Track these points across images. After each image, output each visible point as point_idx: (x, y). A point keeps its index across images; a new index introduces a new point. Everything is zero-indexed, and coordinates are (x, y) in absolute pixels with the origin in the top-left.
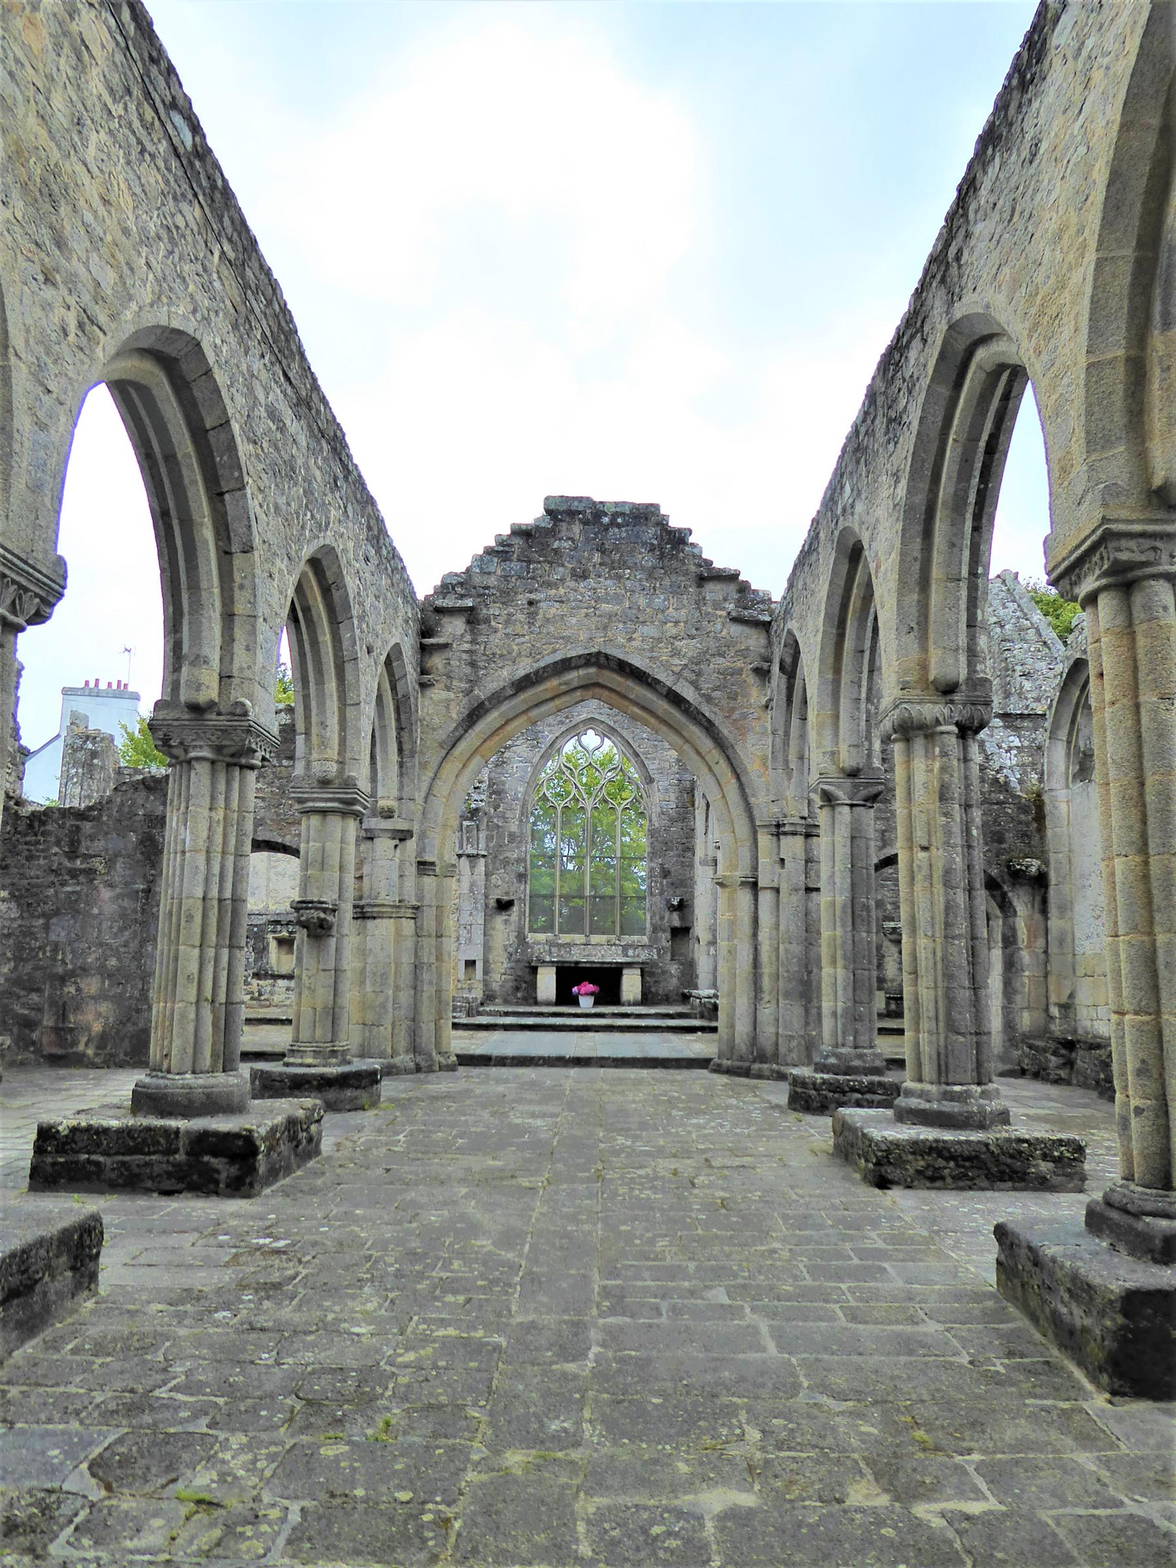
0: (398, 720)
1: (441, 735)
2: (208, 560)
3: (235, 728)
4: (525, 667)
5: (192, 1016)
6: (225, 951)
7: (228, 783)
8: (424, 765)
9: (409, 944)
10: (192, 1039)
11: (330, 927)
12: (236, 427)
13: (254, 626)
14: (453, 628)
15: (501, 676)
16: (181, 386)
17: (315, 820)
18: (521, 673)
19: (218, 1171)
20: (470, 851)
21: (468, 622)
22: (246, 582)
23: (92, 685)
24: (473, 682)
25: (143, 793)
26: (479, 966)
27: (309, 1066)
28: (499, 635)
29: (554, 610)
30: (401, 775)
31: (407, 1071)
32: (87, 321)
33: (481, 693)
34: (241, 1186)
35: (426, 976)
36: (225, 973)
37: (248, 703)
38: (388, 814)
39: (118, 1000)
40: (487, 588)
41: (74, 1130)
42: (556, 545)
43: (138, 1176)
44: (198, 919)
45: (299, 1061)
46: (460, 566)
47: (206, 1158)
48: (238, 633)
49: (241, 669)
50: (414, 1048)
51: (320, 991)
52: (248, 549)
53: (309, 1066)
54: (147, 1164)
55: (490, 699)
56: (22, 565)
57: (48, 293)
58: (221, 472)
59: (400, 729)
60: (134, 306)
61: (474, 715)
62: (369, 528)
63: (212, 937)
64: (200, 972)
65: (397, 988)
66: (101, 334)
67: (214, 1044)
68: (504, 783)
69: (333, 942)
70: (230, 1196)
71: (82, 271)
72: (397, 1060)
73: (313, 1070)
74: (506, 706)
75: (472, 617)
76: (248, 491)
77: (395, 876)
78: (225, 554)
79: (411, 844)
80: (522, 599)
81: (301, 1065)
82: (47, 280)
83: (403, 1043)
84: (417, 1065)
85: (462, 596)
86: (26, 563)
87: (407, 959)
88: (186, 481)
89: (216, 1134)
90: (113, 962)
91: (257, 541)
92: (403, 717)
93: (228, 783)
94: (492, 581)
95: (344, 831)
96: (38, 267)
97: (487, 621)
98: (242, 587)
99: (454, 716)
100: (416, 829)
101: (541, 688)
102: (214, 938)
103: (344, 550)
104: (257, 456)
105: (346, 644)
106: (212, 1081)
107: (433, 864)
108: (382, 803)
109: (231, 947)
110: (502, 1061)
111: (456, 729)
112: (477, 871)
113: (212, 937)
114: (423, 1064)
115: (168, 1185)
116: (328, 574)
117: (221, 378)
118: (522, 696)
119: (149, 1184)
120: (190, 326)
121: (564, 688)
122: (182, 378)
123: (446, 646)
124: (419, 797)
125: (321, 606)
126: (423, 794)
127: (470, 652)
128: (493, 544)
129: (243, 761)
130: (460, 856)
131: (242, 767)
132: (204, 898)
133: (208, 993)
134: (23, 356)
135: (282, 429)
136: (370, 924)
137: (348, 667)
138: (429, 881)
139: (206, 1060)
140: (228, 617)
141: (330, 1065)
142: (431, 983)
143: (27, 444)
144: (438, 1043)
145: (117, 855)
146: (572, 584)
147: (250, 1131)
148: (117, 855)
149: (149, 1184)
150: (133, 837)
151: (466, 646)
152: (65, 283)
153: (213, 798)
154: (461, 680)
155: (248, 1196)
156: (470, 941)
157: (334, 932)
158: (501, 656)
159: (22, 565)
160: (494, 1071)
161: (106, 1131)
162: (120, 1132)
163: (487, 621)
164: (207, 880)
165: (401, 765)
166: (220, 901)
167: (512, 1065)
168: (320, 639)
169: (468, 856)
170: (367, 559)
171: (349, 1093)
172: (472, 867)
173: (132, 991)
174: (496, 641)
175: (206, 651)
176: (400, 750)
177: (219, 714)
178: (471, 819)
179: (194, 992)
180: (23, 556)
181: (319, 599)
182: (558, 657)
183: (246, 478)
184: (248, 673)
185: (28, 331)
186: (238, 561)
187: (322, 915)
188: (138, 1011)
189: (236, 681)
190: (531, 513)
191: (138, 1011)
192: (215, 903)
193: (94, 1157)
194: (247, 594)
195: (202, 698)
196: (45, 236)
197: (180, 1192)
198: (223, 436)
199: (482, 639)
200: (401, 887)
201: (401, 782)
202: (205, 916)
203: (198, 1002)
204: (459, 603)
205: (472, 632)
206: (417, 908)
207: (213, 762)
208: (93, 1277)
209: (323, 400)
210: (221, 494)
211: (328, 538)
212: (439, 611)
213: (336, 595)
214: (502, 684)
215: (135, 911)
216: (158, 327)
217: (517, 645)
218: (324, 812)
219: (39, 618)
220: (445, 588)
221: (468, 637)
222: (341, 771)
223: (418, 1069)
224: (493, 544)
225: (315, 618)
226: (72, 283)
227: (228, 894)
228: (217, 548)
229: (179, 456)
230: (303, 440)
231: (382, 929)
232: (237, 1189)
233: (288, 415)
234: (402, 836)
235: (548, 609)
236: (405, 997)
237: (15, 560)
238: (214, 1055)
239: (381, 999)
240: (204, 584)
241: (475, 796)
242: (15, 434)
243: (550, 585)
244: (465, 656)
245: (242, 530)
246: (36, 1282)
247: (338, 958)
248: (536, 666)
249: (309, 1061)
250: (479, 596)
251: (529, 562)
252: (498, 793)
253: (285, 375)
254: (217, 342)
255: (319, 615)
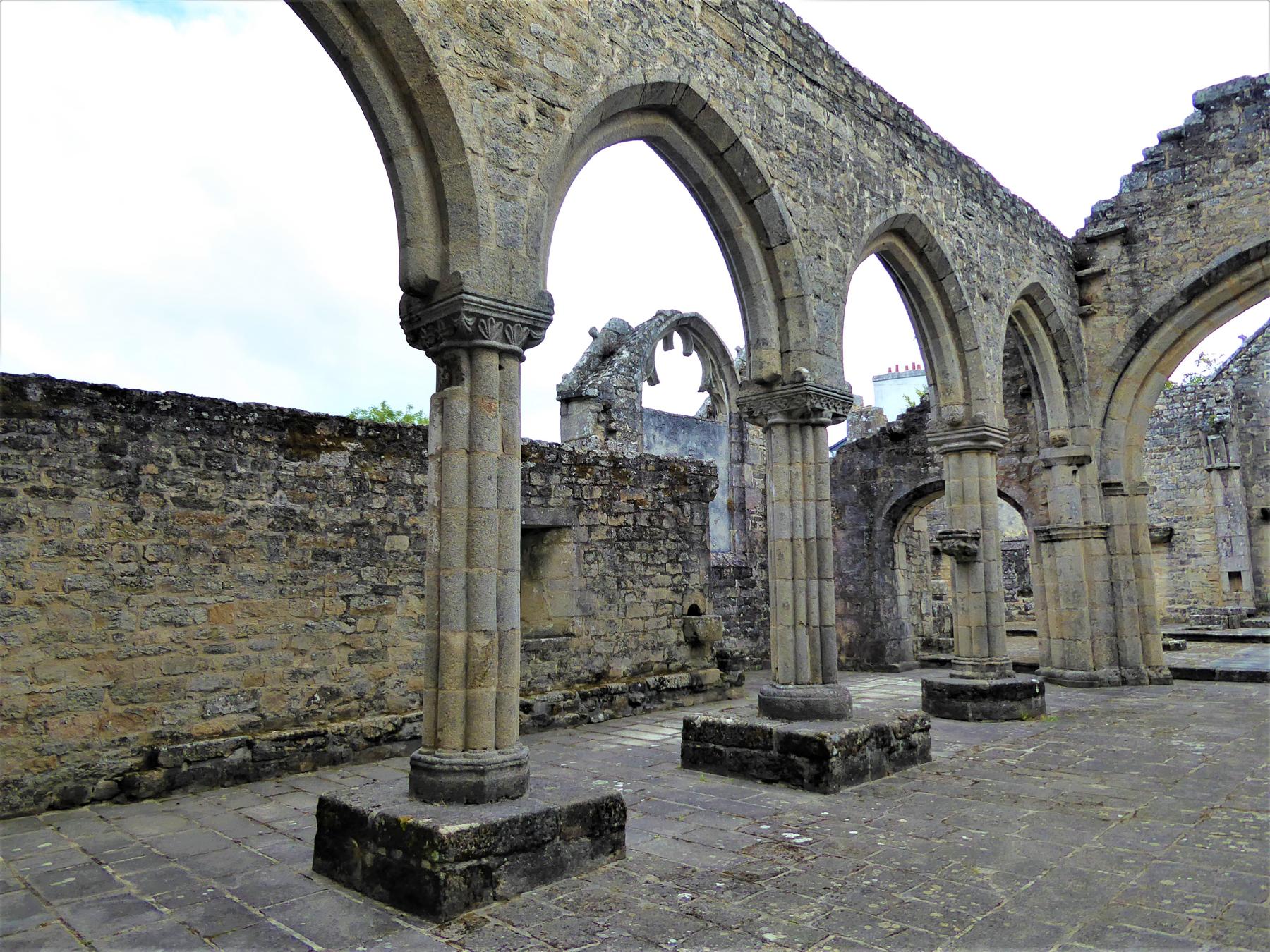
0: (1057, 354)
1: (1110, 359)
2: (753, 259)
3: (796, 394)
4: (1193, 273)
5: (791, 636)
6: (814, 585)
7: (803, 442)
8: (1095, 392)
9: (1102, 563)
10: (792, 656)
11: (975, 554)
12: (748, 143)
13: (803, 304)
14: (1109, 253)
15: (1167, 289)
16: (688, 126)
17: (953, 459)
18: (1190, 280)
19: (801, 768)
20: (1219, 464)
21: (1124, 244)
22: (790, 269)
23: (894, 370)
24: (1137, 302)
25: (858, 453)
26: (1247, 579)
27: (968, 678)
28: (1159, 248)
29: (1221, 205)
30: (1070, 404)
31: (1111, 683)
32: (546, 108)
33: (1147, 310)
34: (819, 782)
35: (1124, 593)
36: (816, 601)
37: (805, 370)
38: (1062, 443)
39: (858, 618)
40: (1141, 204)
41: (705, 724)
42: (1212, 138)
43: (746, 765)
44: (788, 556)
45: (960, 673)
46: (1110, 190)
47: (792, 757)
48: (791, 314)
49: (797, 343)
50: (1119, 661)
51: (973, 611)
52: (785, 241)
53: (968, 678)
54: (752, 756)
55: (1158, 314)
56: (502, 305)
57: (501, 98)
58: (745, 184)
59: (1061, 362)
60: (601, 79)
61: (1144, 334)
62: (967, 185)
63: (802, 571)
64: (795, 601)
65: (1093, 605)
66: (565, 113)
67: (812, 661)
68: (1254, 392)
69: (980, 567)
70: (812, 790)
71: (537, 70)
72: (1101, 673)
73: (967, 682)
74: (1179, 318)
75: (1127, 238)
76: (775, 192)
77: (1077, 500)
78: (768, 250)
79: (1092, 470)
80: (1180, 205)
81: (962, 677)
82: (498, 88)
83: (1105, 656)
84: (1123, 677)
85: (1114, 220)
86: (505, 303)
87: (1100, 579)
88: (718, 200)
89: (797, 737)
90: (851, 588)
91: (794, 230)
92: (1061, 349)
93: (803, 442)
94: (1145, 196)
95: (981, 466)
96: (487, 82)
97: (1144, 237)
98: (786, 274)
99: (1121, 338)
100: (1094, 453)
101: (1219, 289)
102: (803, 572)
103: (933, 214)
104: (782, 159)
105: (952, 297)
106: (811, 691)
107: (1119, 484)
108: (1053, 434)
109: (820, 578)
110: (1228, 676)
111: (1125, 350)
112: (1230, 483)
113: (802, 571)
114: (1129, 677)
115: (768, 774)
116: (917, 239)
117: (718, 106)
118: (1197, 304)
119: (755, 773)
120: (674, 75)
121: (1248, 284)
122: (686, 119)
123: (1102, 273)
124: (1095, 423)
125: (919, 270)
126: (1099, 419)
127: (1130, 272)
128: (1141, 159)
129: (813, 420)
130: (1209, 470)
131: (814, 426)
132: (792, 540)
133: (802, 617)
134: (480, 151)
135: (815, 126)
136: (1057, 546)
137: (960, 318)
138: (1115, 501)
139: (807, 674)
140: (780, 301)
141: (987, 678)
142: (1131, 599)
143: (493, 215)
144: (1146, 658)
145: (845, 503)
146: (1238, 173)
147: (823, 737)
148: (845, 503)
149: (755, 773)
150: (854, 488)
151: (1125, 268)
152: (518, 84)
153: (791, 455)
154: (1123, 302)
155: (825, 793)
156: (1231, 553)
157: (980, 557)
158: (1165, 268)
159: (502, 305)
160: (1216, 685)
161: (723, 727)
162: (736, 729)
163: (1144, 237)
164: (792, 524)
165: (1068, 395)
166: (806, 540)
167: (1239, 681)
168: (925, 299)
169: (1218, 469)
170: (968, 215)
171: (1004, 704)
172: (1225, 480)
173: (867, 610)
174: (1156, 256)
175: (764, 334)
176: (1066, 382)
177: (784, 384)
178: (1217, 433)
179: (790, 617)
180: (501, 298)
181: (915, 263)
182: (1231, 253)
183: (770, 182)
184: (804, 346)
185: (482, 131)
186: (779, 253)
187: (963, 544)
188: (873, 627)
189: (794, 354)
190: (1179, 114)
191: (873, 627)
192: (802, 543)
193: (718, 747)
194: (793, 278)
195: (764, 374)
196: (491, 57)
197: (776, 782)
198: (737, 154)
199: (1140, 256)
200: (1085, 510)
201: (1071, 411)
202: (794, 554)
203: (794, 626)
204: (1111, 228)
205: (1129, 252)
206: (1107, 528)
207: (787, 425)
208: (618, 845)
209: (874, 88)
210: (752, 202)
211: (904, 207)
212: (1092, 241)
213: (931, 256)
214: (1169, 296)
215: (862, 547)
216: (633, 87)
217: (1178, 255)
218: (959, 451)
219: (532, 341)
220: (1096, 217)
221: (1126, 259)
222: (968, 413)
223: (1124, 682)
224: (1141, 159)
225: (915, 281)
226: (526, 82)
227: (812, 534)
228: (761, 247)
229: (706, 182)
230: (847, 131)
231: (1069, 551)
232: (817, 785)
233: (820, 114)
234: (1081, 462)
235: (1212, 207)
236: (1103, 614)
237: (493, 303)
238: (814, 670)
239: (1075, 615)
240: (753, 280)
241: (1218, 410)
242: (481, 211)
243: (1210, 182)
244: (1124, 278)
245: (777, 226)
246: (545, 843)
247: (987, 582)
248: (1207, 269)
249: (969, 673)
250: (1132, 214)
251: (1184, 165)
252: (1248, 402)
253: (810, 80)
254: (711, 80)
255: (920, 279)
